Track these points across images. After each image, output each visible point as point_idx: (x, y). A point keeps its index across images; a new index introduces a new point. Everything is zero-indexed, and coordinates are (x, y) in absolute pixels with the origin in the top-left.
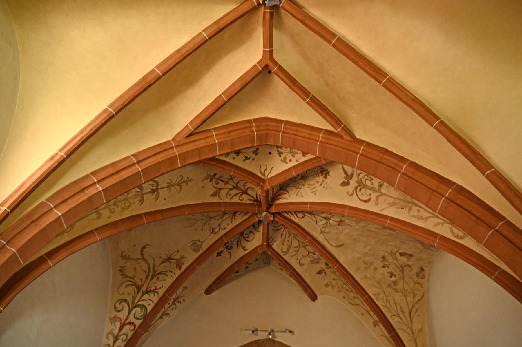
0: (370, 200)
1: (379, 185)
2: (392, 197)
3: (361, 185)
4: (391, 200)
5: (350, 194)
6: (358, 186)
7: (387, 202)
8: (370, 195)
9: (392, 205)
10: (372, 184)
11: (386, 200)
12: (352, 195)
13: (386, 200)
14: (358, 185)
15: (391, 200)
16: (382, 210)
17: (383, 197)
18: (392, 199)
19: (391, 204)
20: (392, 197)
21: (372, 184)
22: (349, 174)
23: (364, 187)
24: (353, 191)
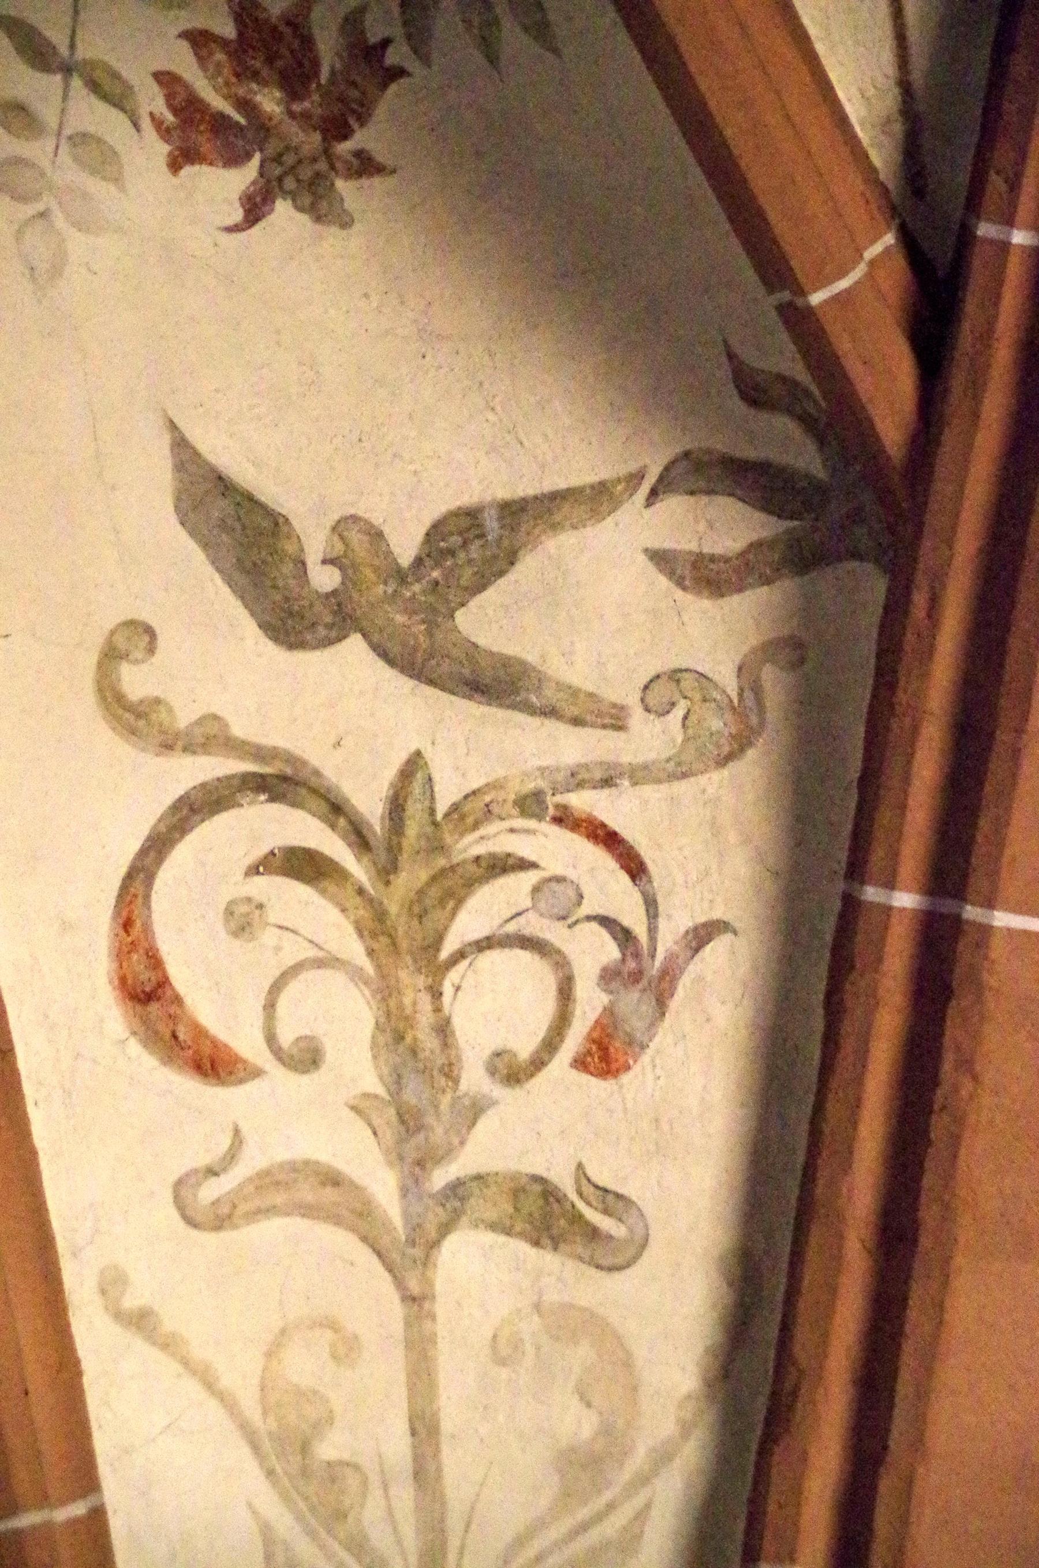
0: (212, 1064)
1: (549, 1193)
2: (424, 1429)
3: (402, 873)
4: (369, 1430)
5: (136, 681)
6: (336, 810)
7: (303, 1365)
8: (306, 1058)
9: (290, 1448)
10: (513, 1072)
11: (346, 1349)
12: (134, 719)
13: (346, 1349)
14: (370, 803)
15: (369, 1430)
16: (141, 1322)
17: (368, 1297)
18: (397, 1446)
19: (305, 1448)
20: (424, 1429)
21: (513, 1072)
22: (489, 622)
23: (376, 927)
24: (209, 736)
